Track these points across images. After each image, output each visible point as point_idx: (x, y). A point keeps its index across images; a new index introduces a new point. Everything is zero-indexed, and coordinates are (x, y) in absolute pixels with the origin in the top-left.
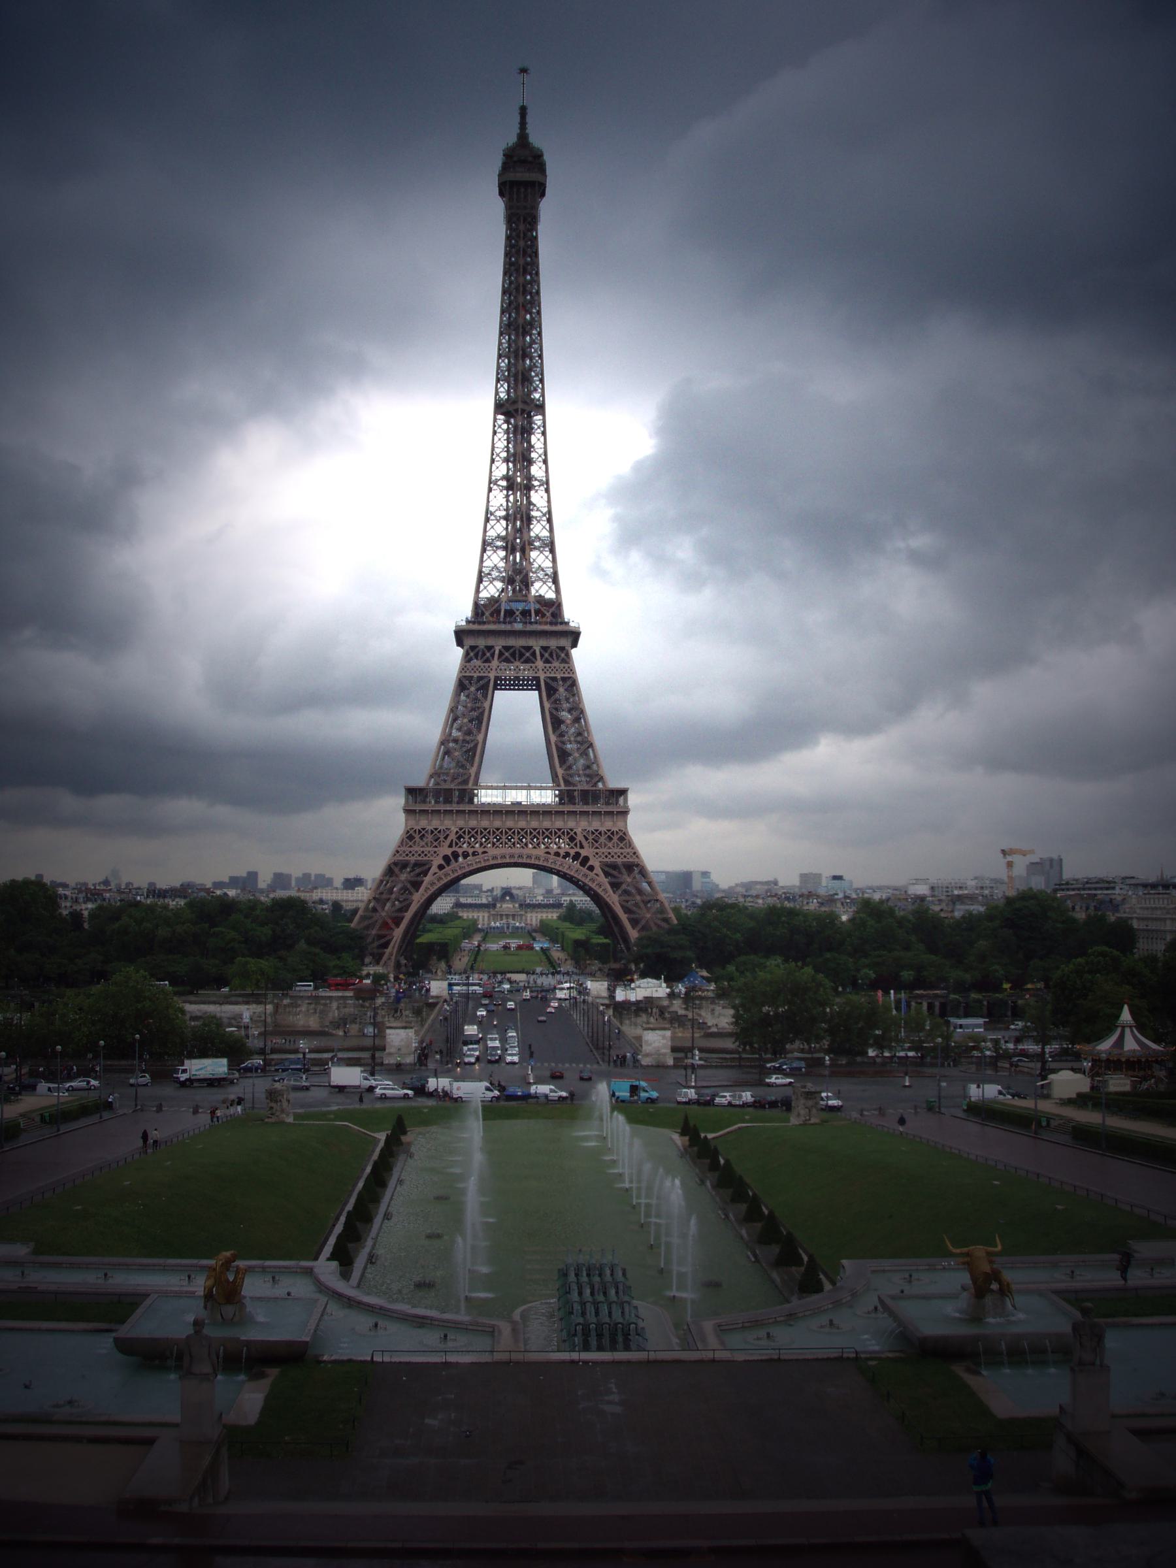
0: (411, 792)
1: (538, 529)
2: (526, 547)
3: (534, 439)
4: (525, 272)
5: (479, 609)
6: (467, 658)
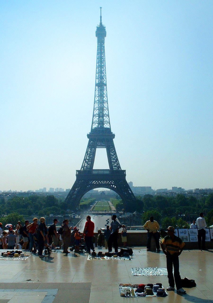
1: (105, 112)
2: (103, 116)
3: (104, 92)
4: (102, 54)
5: (92, 130)
6: (90, 142)
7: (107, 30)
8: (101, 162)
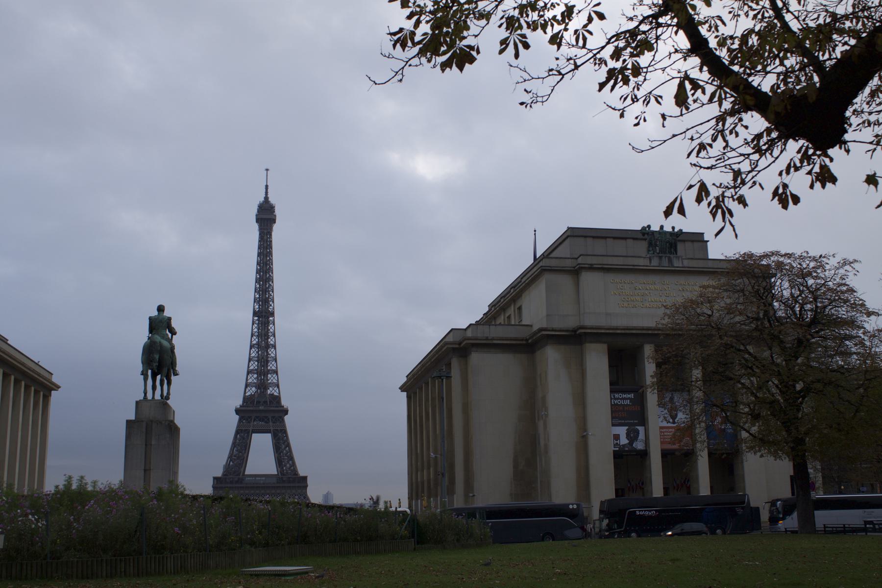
0: (215, 478)
1: (271, 366)
6: (240, 421)
7: (278, 212)
8: (261, 459)
